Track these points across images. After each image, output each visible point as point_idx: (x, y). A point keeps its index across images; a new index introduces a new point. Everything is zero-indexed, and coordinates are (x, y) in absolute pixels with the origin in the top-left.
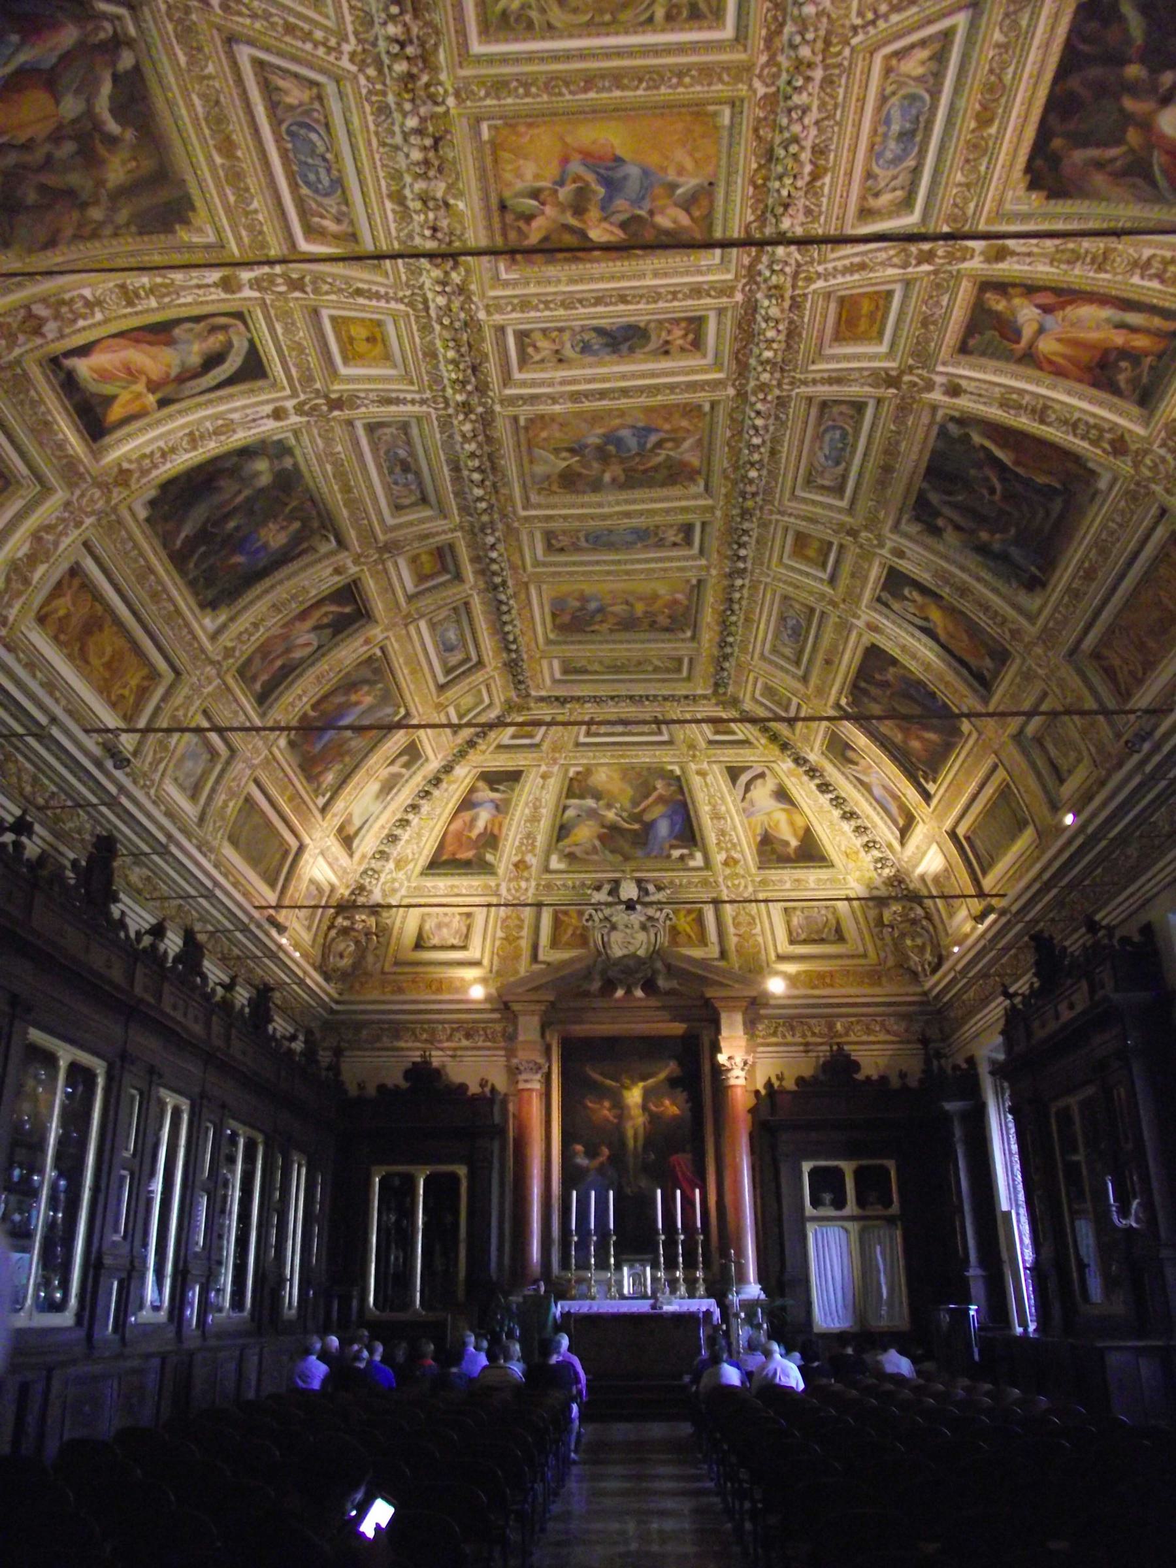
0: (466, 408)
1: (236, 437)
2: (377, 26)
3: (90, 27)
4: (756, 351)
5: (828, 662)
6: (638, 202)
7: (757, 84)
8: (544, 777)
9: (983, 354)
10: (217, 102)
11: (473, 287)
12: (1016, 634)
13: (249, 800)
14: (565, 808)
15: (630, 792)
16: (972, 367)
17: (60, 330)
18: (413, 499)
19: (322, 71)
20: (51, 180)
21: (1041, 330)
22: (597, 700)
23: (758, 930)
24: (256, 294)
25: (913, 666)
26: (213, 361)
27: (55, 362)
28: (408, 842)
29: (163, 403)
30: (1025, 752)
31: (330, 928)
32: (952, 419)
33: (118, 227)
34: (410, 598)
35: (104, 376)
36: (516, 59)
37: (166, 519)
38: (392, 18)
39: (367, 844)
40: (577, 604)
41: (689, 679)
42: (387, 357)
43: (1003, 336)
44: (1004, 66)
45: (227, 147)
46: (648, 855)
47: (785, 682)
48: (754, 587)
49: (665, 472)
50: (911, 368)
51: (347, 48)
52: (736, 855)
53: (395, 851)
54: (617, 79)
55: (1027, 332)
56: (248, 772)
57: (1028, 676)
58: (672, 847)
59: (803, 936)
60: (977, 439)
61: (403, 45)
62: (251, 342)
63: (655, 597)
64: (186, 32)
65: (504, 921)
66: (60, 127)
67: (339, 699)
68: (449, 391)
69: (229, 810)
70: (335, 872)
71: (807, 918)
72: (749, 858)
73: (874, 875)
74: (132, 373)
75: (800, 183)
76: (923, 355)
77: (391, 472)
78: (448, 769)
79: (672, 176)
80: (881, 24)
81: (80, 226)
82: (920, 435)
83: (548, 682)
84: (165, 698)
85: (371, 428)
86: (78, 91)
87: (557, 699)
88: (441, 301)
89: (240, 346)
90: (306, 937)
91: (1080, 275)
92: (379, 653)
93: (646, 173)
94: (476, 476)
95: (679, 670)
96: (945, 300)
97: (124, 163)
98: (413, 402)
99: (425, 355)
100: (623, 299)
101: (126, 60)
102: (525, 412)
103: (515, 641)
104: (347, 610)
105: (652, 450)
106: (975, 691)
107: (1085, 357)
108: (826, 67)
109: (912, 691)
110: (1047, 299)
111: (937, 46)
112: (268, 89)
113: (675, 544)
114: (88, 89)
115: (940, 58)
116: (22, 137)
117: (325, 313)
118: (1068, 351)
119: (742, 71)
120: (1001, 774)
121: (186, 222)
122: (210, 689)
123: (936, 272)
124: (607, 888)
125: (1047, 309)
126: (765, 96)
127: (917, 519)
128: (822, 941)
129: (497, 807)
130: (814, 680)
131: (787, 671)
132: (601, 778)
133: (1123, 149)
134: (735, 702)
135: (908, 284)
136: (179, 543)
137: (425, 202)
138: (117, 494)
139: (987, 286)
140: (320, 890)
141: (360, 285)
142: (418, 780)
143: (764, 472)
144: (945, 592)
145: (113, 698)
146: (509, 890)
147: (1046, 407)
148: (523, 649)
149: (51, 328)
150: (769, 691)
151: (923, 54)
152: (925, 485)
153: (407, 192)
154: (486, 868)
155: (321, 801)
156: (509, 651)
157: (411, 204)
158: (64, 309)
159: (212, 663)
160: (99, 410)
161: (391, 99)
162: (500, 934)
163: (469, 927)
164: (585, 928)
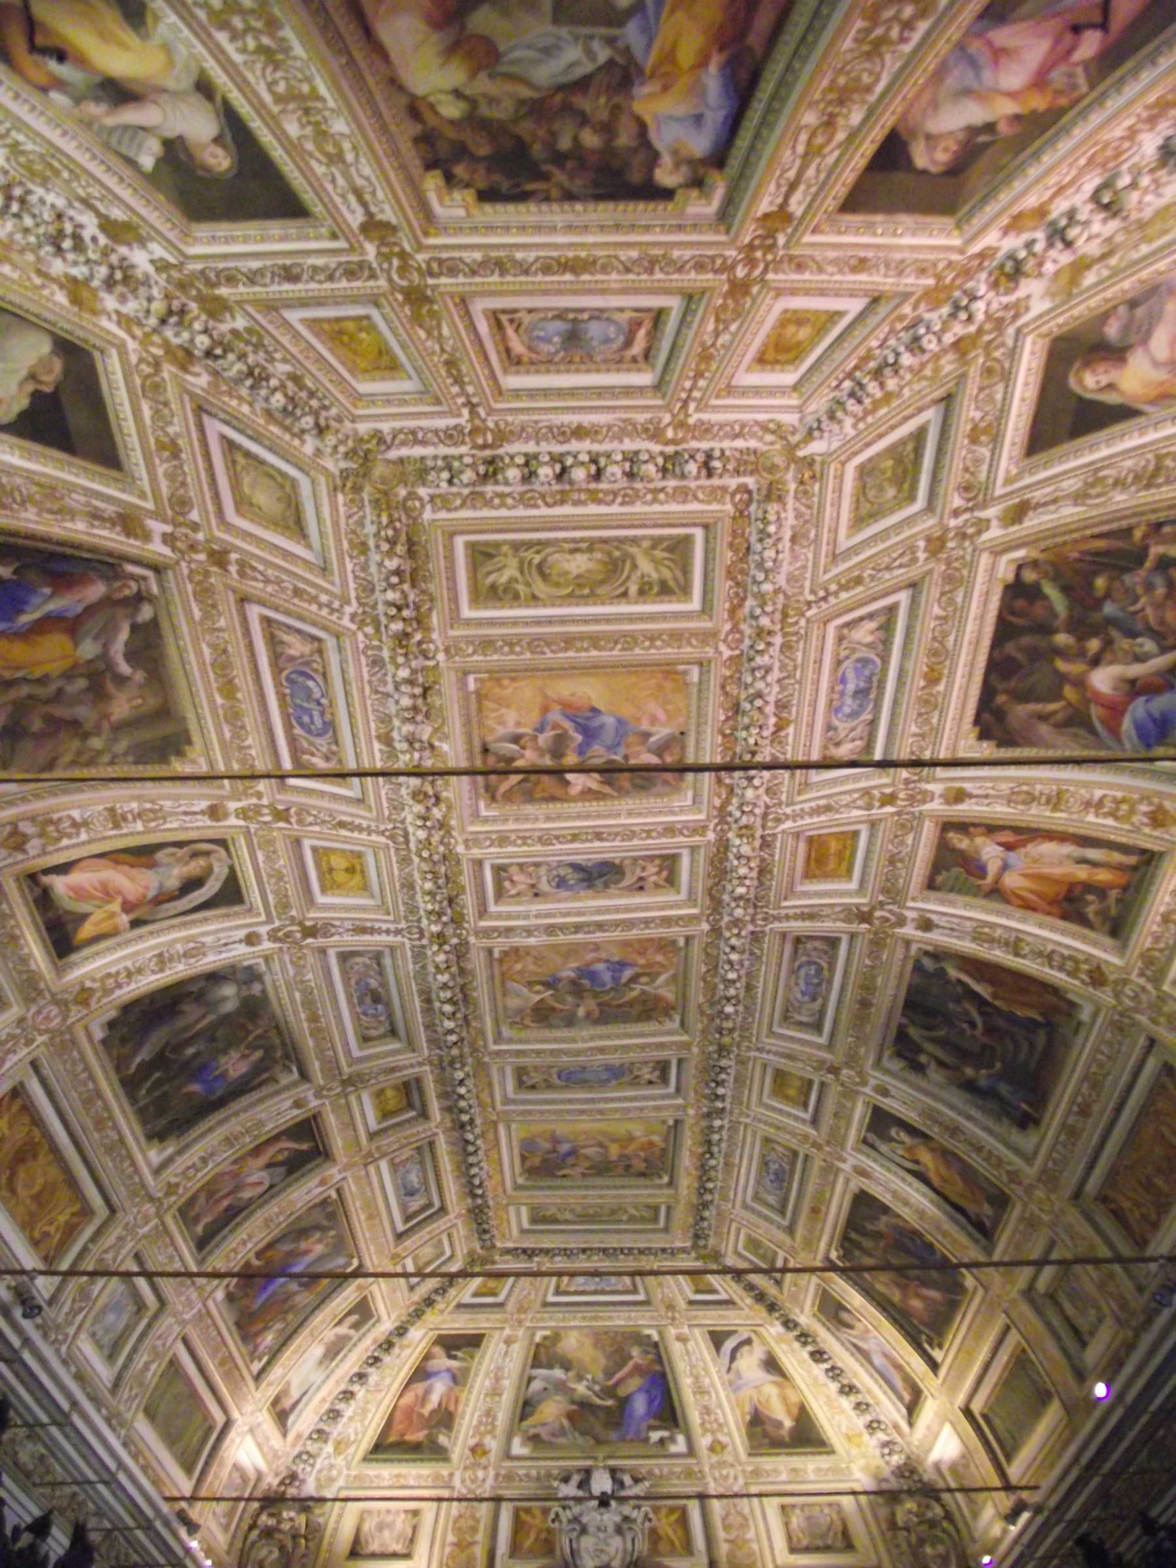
0: (440, 938)
1: (206, 960)
2: (377, 593)
3: (117, 584)
4: (729, 887)
5: (815, 1210)
6: (611, 748)
7: (722, 647)
8: (508, 1342)
9: (951, 890)
10: (225, 651)
11: (453, 823)
12: (1014, 1177)
13: (174, 1363)
14: (530, 1380)
15: (603, 1361)
16: (942, 902)
17: (44, 846)
18: (382, 1030)
19: (325, 628)
20: (59, 711)
21: (1005, 867)
22: (567, 1253)
23: (751, 1534)
24: (242, 823)
25: (905, 1213)
26: (192, 884)
27: (33, 877)
28: (351, 1419)
29: (135, 924)
30: (1039, 1312)
31: (251, 1528)
32: (926, 953)
33: (114, 756)
34: (372, 1136)
35: (80, 893)
36: (502, 622)
37: (123, 1041)
38: (393, 587)
39: (304, 1421)
40: (547, 1146)
41: (666, 1230)
42: (365, 888)
43: (969, 873)
44: (945, 635)
45: (229, 689)
46: (622, 1439)
47: (770, 1233)
48: (733, 1128)
49: (638, 1008)
50: (882, 904)
51: (348, 610)
52: (724, 1439)
53: (336, 1431)
54: (595, 641)
55: (993, 868)
56: (177, 1329)
57: (1031, 1223)
59: (805, 1542)
60: (953, 973)
61: (399, 609)
62: (232, 868)
63: (631, 1138)
64: (204, 593)
65: (456, 1520)
66: (75, 666)
67: (286, 1247)
68: (425, 922)
69: (149, 1375)
70: (264, 1455)
71: (808, 1519)
73: (880, 1462)
74: (108, 893)
75: (766, 733)
76: (893, 892)
77: (361, 1003)
78: (401, 1331)
79: (645, 726)
80: (832, 600)
81: (79, 753)
82: (895, 970)
83: (515, 1232)
84: (93, 1239)
85: (344, 957)
86: (96, 638)
87: (524, 1251)
88: (422, 834)
89: (220, 872)
90: (222, 1540)
91: (1037, 815)
92: (334, 1195)
93: (620, 722)
94: (448, 1008)
95: (656, 1219)
96: (910, 839)
97: (130, 700)
98: (388, 932)
99: (403, 886)
100: (599, 836)
101: (146, 613)
102: (500, 944)
103: (480, 1186)
104: (304, 1146)
105: (627, 984)
106: (977, 1241)
107: (1051, 891)
108: (785, 635)
109: (910, 1244)
110: (1008, 837)
111: (882, 619)
112: (273, 641)
113: (650, 1082)
114: (106, 634)
115: (887, 627)
116: (38, 673)
117: (307, 844)
118: (1033, 886)
119: (708, 637)
120: (1014, 1338)
121: (180, 753)
122: (146, 1229)
123: (899, 813)
124: (576, 1479)
125: (1009, 847)
126: (731, 658)
127: (899, 1055)
130: (800, 1231)
131: (772, 1222)
132: (572, 1344)
133: (1062, 703)
134: (716, 1256)
135: (873, 824)
136: (133, 1067)
137: (411, 744)
138: (75, 1012)
139: (947, 826)
140: (244, 1478)
141: (344, 818)
142: (366, 1345)
143: (741, 1008)
144: (934, 1131)
145: (37, 1234)
147: (1018, 940)
148: (490, 1195)
149: (33, 846)
150: (754, 1244)
151: (873, 625)
152: (904, 1021)
153: (395, 735)
154: (439, 1453)
155: (256, 1366)
156: (474, 1196)
157: (398, 746)
158: (51, 828)
159: (152, 1199)
160: (70, 927)
161: (386, 654)
163: (415, 1529)
164: (549, 1531)
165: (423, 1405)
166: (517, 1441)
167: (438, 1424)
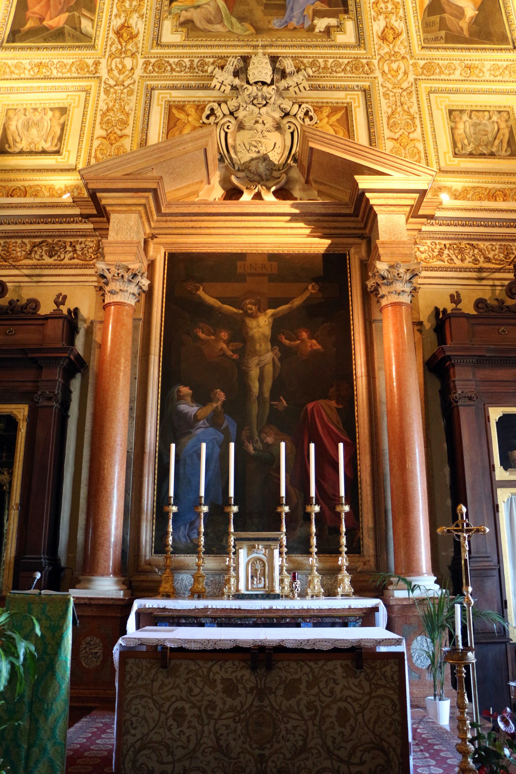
23: (417, 134)
65: (104, 114)
71: (475, 125)
124: (232, 65)
128: (492, 155)
146: (110, 71)
162: (99, 132)
166: (168, 25)
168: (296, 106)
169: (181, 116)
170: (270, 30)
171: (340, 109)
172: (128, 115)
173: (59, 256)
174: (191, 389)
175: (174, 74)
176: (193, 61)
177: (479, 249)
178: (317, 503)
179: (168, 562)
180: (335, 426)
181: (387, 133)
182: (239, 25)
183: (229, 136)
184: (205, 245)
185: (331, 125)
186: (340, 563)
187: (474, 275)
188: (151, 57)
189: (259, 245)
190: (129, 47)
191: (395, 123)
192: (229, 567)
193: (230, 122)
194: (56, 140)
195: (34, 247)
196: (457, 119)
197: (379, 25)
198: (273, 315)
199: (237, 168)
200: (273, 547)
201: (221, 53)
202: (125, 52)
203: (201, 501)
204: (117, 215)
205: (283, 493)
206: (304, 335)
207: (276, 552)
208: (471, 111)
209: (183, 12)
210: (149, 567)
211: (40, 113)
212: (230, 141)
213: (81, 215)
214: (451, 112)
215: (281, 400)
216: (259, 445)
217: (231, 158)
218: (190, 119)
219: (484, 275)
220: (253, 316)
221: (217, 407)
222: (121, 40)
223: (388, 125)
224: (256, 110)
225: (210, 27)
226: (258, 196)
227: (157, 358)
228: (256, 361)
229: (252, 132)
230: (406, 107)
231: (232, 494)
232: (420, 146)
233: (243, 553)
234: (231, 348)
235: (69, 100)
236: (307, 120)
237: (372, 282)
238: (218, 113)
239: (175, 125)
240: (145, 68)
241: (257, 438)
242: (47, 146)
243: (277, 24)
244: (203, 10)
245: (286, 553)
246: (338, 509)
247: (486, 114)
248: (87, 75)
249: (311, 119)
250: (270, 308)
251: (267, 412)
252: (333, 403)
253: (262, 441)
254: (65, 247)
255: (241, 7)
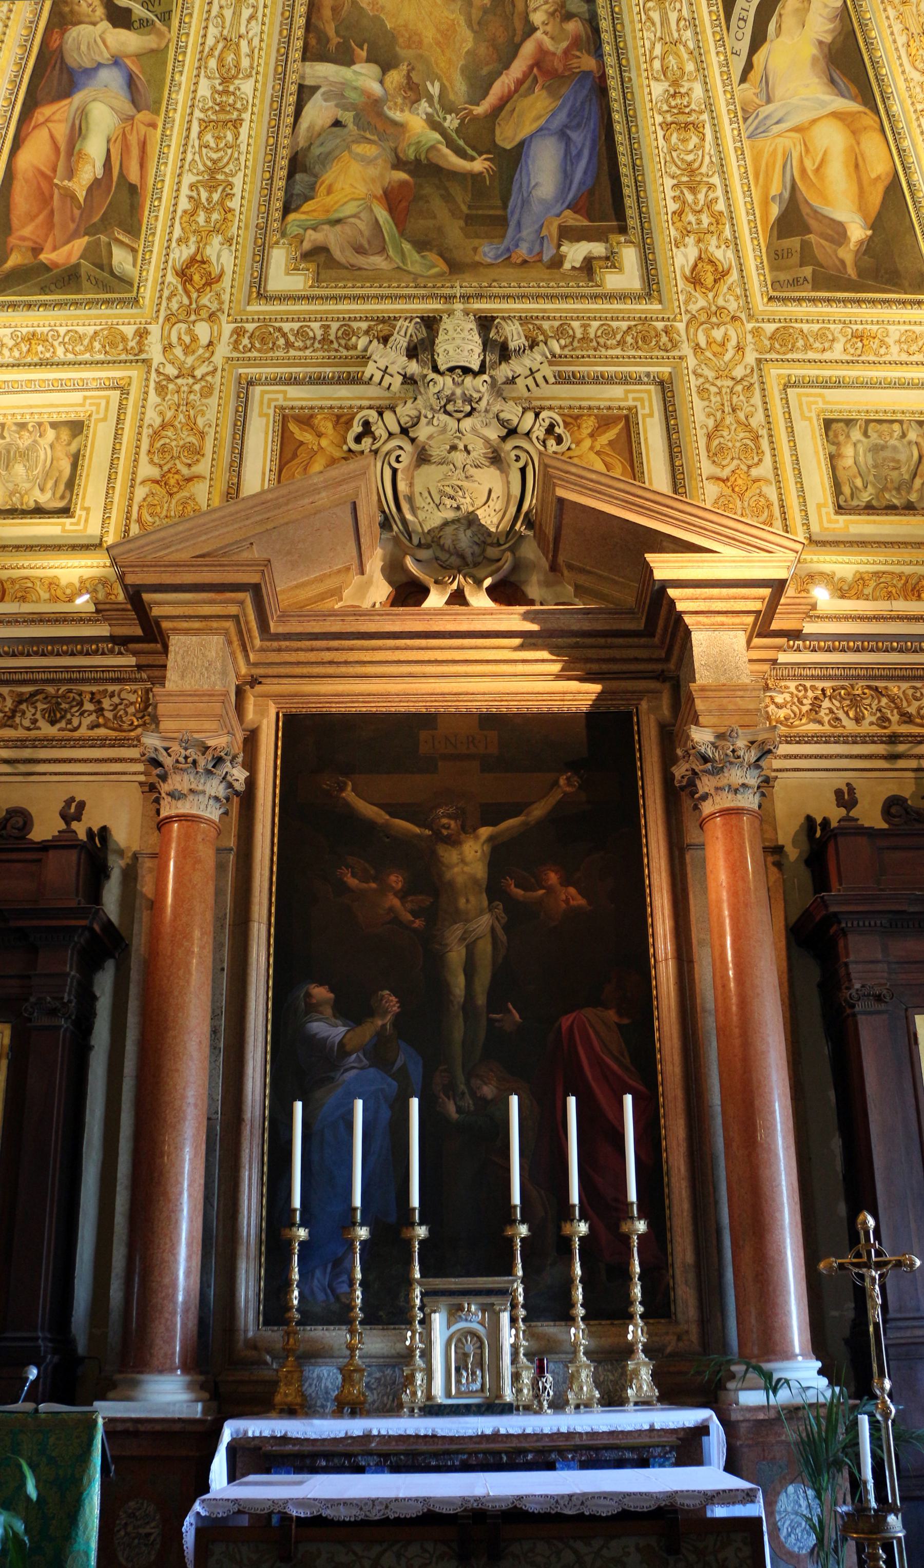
14: (304, 93)
15: (466, 40)
23: (765, 469)
52: (723, 255)
58: (569, 234)
59: (866, 497)
65: (156, 435)
71: (876, 449)
72: (751, 263)
129: (131, 82)
146: (167, 348)
162: (146, 470)
163: (76, 460)
165: (71, 174)
166: (279, 257)
167: (105, 224)
168: (530, 416)
169: (307, 437)
170: (478, 265)
171: (616, 419)
172: (202, 435)
173: (69, 722)
174: (332, 990)
175: (292, 353)
176: (329, 326)
177: (888, 696)
178: (583, 1217)
179: (291, 1341)
180: (616, 1059)
181: (707, 467)
182: (416, 256)
183: (400, 475)
184: (355, 698)
185: (598, 453)
186: (630, 1337)
187: (881, 749)
188: (247, 321)
189: (462, 697)
190: (205, 301)
191: (721, 448)
192: (411, 1350)
193: (401, 448)
194: (62, 487)
195: (20, 702)
196: (841, 438)
197: (685, 256)
198: (490, 839)
199: (415, 541)
200: (497, 1308)
201: (383, 311)
202: (197, 311)
203: (354, 1216)
204: (183, 638)
205: (516, 1199)
206: (553, 878)
207: (505, 1317)
208: (868, 422)
209: (310, 232)
210: (254, 1353)
211: (30, 433)
212: (402, 486)
213: (113, 639)
214: (828, 424)
215: (509, 1011)
216: (468, 1103)
217: (404, 521)
218: (324, 443)
219: (901, 748)
220: (454, 842)
221: (384, 1026)
222: (189, 286)
223: (708, 451)
224: (452, 424)
225: (361, 260)
226: (458, 598)
227: (264, 928)
228: (459, 933)
229: (444, 468)
230: (741, 415)
231: (415, 1201)
232: (771, 493)
233: (438, 1320)
234: (409, 906)
235: (87, 407)
236: (551, 442)
237: (684, 768)
238: (379, 430)
239: (295, 456)
240: (236, 341)
241: (462, 1087)
242: (45, 498)
243: (491, 254)
244: (347, 229)
245: (524, 1320)
246: (625, 1228)
247: (896, 427)
248: (123, 357)
249: (559, 440)
250: (485, 824)
251: (482, 1035)
252: (611, 1015)
253: (473, 1094)
254: (81, 704)
255: (421, 222)
